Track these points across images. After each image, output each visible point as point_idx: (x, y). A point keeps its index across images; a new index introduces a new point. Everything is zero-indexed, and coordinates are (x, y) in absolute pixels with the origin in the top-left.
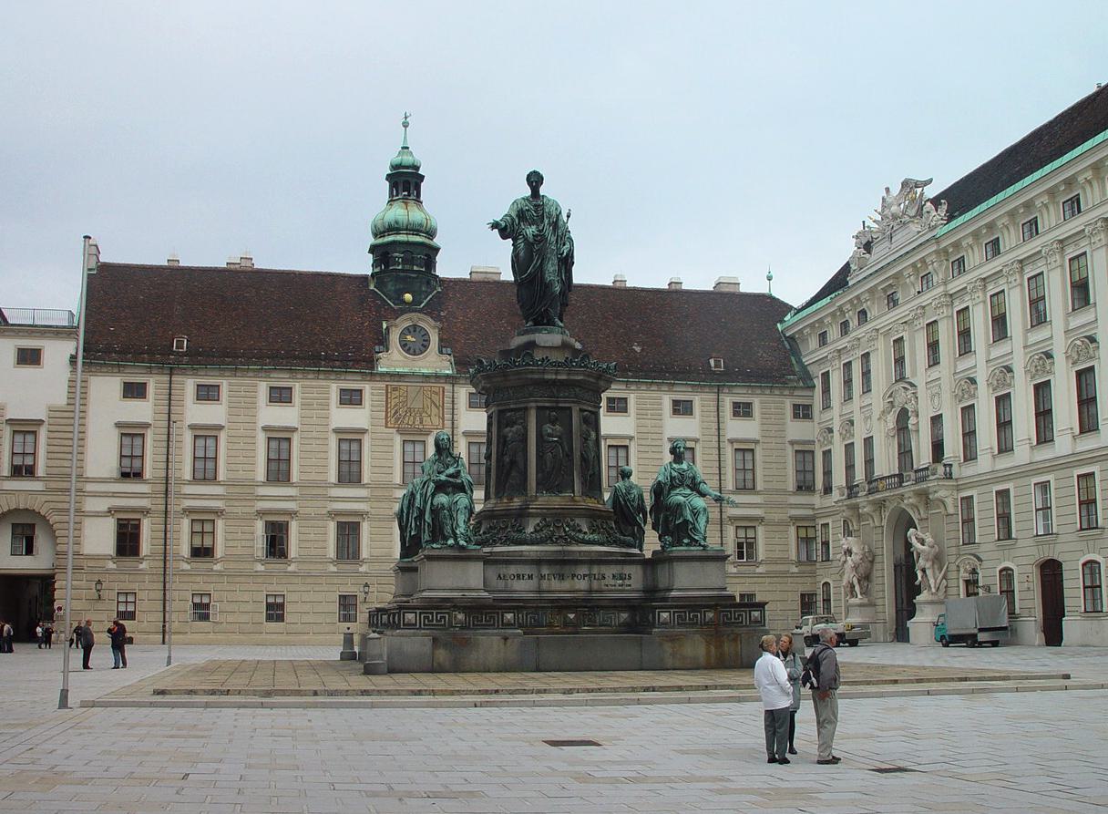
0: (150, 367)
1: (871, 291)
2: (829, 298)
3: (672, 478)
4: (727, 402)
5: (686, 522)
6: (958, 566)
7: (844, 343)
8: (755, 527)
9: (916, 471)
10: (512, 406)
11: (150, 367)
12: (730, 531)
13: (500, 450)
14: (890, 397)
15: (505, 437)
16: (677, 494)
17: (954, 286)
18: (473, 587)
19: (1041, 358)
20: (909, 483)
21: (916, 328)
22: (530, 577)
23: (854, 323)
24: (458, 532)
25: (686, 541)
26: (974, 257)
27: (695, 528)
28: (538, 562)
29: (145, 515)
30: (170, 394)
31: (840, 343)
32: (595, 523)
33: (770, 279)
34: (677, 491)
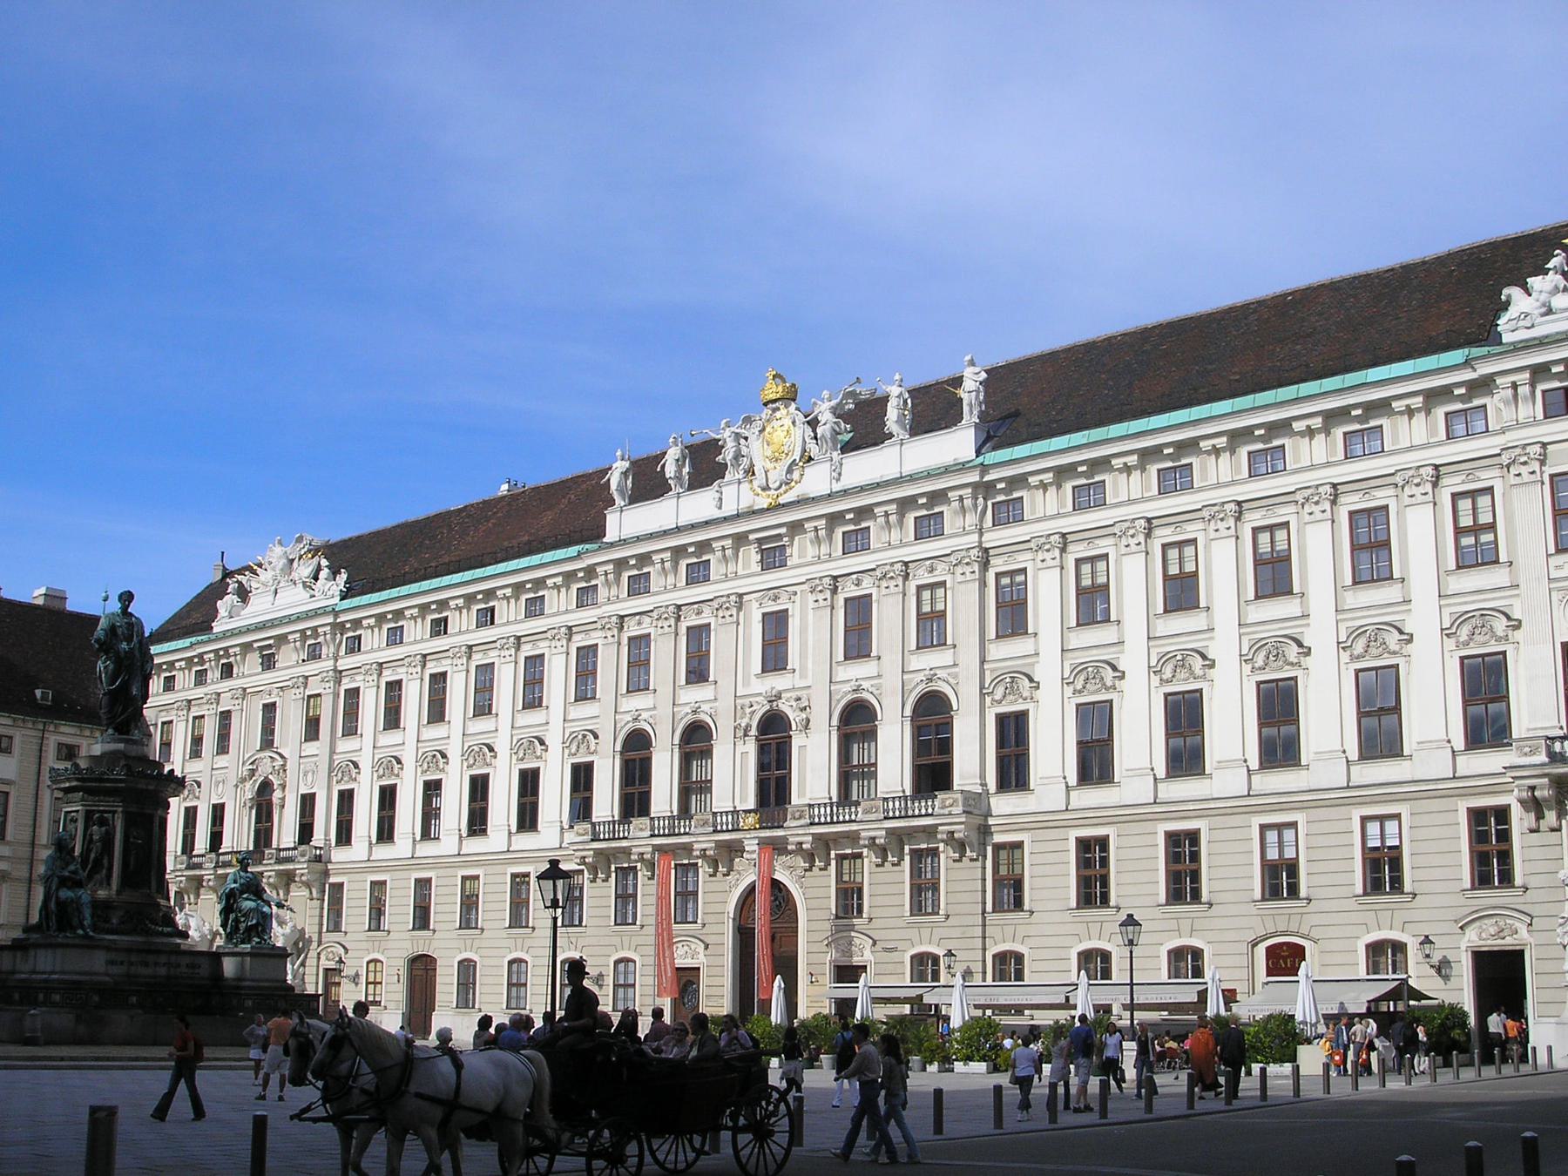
1: (247, 647)
2: (190, 640)
4: (52, 741)
6: (319, 954)
7: (199, 692)
9: (280, 850)
10: (101, 808)
14: (251, 763)
15: (91, 835)
16: (247, 899)
17: (344, 663)
19: (434, 756)
20: (272, 861)
21: (294, 697)
22: (122, 963)
23: (214, 674)
25: (258, 940)
26: (373, 640)
28: (129, 951)
31: (193, 691)
33: (105, 600)
34: (245, 896)
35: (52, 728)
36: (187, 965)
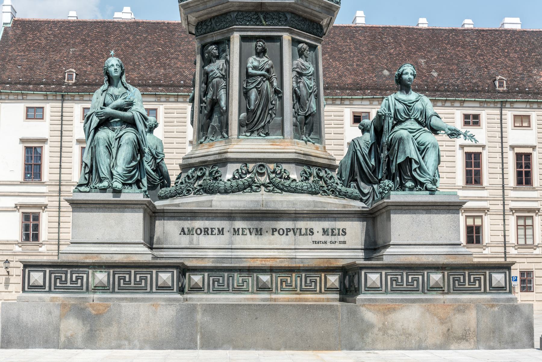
0: (46, 95)
3: (396, 111)
5: (409, 160)
8: (532, 216)
11: (46, 95)
12: (512, 220)
13: (203, 90)
15: (207, 74)
18: (129, 241)
22: (221, 232)
24: (114, 172)
25: (409, 184)
27: (420, 168)
29: (43, 210)
30: (62, 116)
32: (307, 170)
35: (508, 105)
36: (325, 232)
